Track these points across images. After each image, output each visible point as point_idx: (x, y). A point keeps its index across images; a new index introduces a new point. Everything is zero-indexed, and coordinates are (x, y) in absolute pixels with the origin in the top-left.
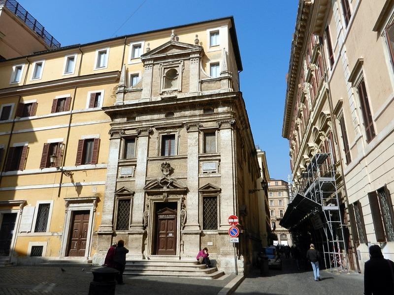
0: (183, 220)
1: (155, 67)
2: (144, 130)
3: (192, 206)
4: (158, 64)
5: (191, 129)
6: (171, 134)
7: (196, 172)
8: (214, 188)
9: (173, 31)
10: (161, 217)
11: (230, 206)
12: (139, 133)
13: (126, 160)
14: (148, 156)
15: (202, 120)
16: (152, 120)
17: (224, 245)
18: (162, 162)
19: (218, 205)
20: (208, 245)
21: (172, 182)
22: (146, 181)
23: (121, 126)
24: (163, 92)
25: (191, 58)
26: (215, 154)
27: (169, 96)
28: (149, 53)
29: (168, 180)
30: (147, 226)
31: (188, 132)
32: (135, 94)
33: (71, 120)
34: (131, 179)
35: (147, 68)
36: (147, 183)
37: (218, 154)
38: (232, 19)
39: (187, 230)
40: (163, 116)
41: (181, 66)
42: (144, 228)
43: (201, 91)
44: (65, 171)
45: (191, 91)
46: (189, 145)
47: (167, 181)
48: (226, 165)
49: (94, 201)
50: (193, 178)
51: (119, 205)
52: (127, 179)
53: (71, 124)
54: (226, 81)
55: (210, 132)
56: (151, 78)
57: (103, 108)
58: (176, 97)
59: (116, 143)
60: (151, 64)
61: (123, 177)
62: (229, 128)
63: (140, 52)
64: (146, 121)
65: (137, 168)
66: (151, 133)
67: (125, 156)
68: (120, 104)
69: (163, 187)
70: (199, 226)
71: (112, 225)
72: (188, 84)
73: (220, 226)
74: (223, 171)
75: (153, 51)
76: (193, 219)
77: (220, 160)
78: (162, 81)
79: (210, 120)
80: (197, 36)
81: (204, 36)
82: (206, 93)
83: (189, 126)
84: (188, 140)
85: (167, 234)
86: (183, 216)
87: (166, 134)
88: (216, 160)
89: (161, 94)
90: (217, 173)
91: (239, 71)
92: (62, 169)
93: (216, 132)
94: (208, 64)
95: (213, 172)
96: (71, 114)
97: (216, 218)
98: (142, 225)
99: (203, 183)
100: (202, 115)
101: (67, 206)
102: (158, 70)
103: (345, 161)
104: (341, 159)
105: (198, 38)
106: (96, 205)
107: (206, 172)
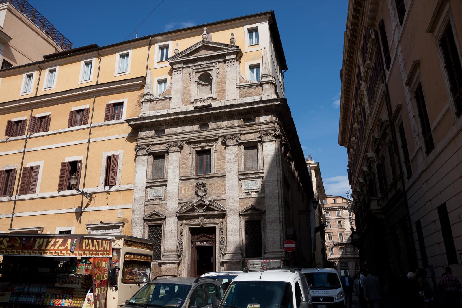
3: (232, 231)
4: (189, 67)
6: (206, 148)
7: (235, 192)
15: (241, 132)
16: (183, 133)
18: (196, 181)
21: (210, 204)
23: (148, 141)
24: (195, 100)
25: (227, 60)
27: (202, 104)
28: (177, 55)
29: (204, 202)
32: (162, 103)
34: (163, 202)
37: (262, 171)
38: (272, 14)
40: (196, 127)
41: (215, 69)
44: (87, 193)
45: (228, 98)
50: (233, 199)
51: (150, 231)
52: (157, 202)
53: (90, 139)
55: (251, 145)
57: (127, 121)
58: (210, 106)
59: (143, 160)
61: (152, 199)
64: (176, 134)
66: (181, 148)
68: (146, 115)
70: (241, 254)
72: (224, 90)
73: (265, 253)
75: (181, 53)
79: (251, 131)
84: (227, 155)
86: (222, 243)
87: (200, 149)
88: (259, 177)
91: (283, 71)
92: (83, 192)
96: (90, 128)
100: (242, 126)
103: (406, 175)
104: (402, 173)
107: (248, 192)
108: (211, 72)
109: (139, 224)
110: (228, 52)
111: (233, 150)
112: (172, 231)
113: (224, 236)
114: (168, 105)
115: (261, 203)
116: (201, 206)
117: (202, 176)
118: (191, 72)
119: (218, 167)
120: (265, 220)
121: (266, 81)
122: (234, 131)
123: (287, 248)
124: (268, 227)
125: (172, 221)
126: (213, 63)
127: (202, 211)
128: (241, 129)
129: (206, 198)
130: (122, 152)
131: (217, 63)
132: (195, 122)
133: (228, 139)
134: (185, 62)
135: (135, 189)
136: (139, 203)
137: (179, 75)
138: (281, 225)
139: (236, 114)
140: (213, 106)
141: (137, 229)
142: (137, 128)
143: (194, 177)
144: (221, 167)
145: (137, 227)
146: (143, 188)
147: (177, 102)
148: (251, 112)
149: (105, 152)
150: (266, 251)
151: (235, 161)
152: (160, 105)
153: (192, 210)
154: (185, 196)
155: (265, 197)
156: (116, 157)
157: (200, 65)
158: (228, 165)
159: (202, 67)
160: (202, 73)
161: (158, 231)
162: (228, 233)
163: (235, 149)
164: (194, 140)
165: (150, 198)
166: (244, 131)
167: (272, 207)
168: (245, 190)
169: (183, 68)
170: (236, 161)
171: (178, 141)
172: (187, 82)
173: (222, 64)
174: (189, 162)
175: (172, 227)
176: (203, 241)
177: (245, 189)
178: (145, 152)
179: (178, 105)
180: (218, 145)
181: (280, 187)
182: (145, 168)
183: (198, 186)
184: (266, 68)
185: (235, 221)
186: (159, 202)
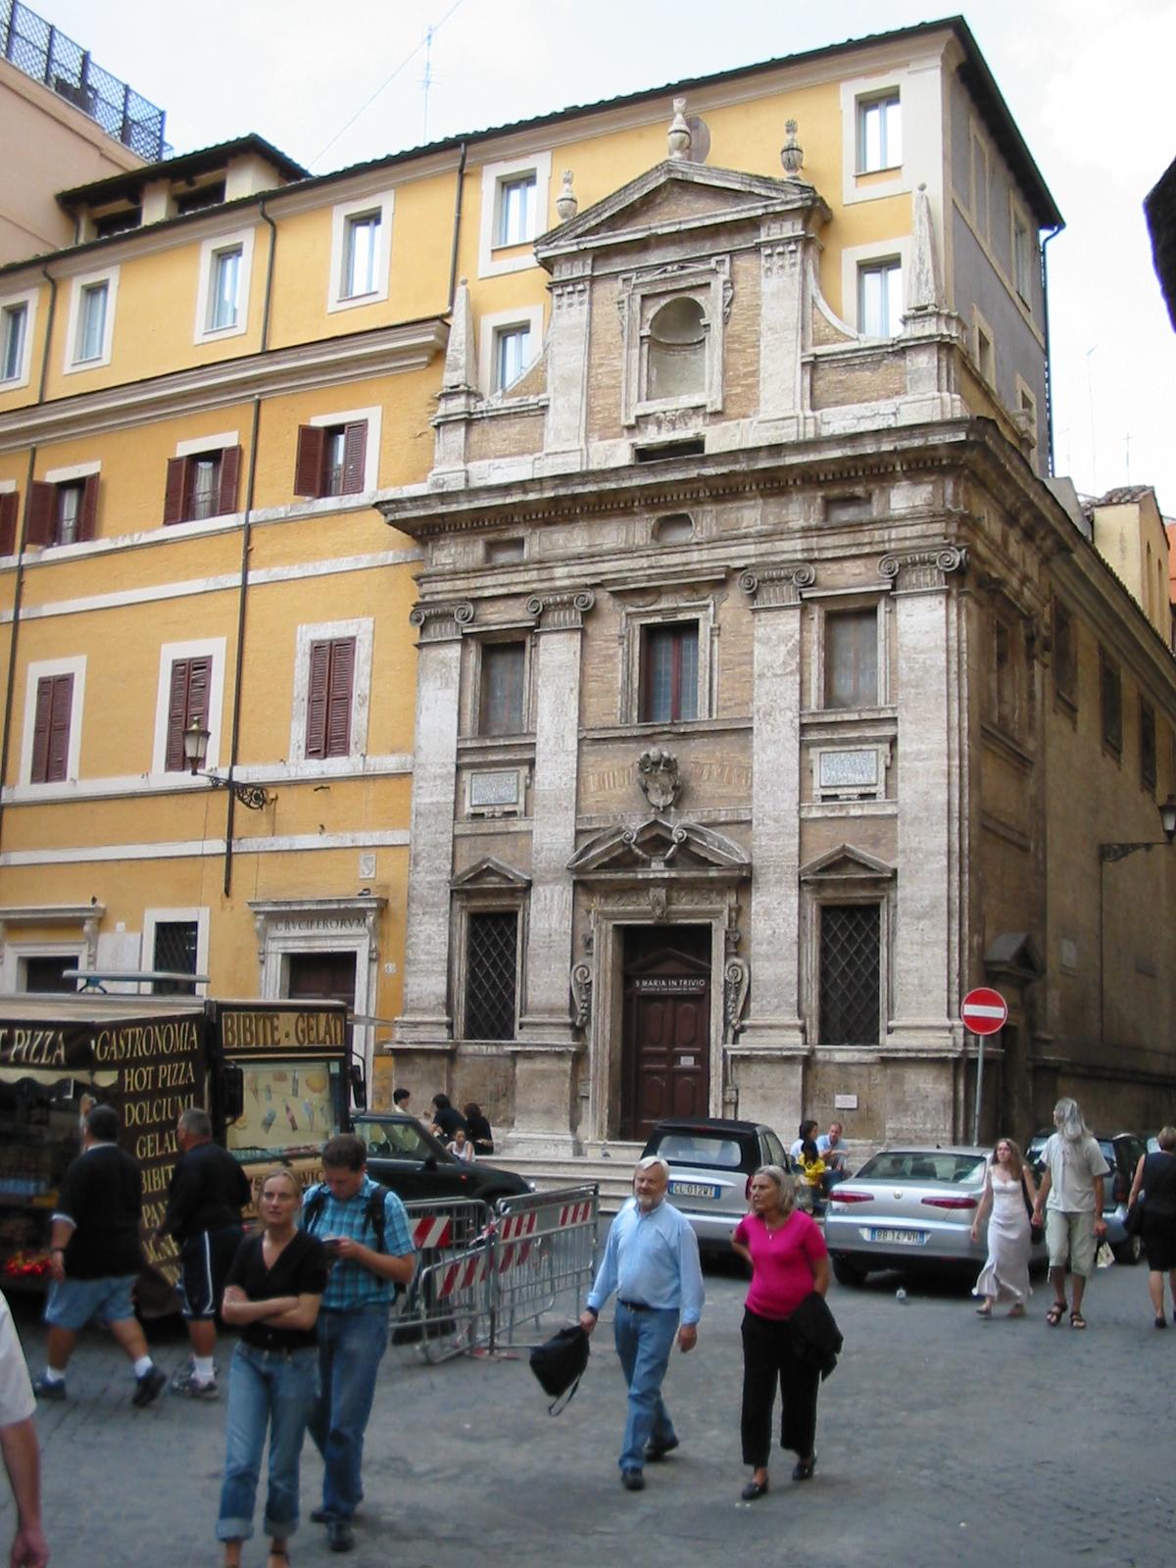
0: (735, 1001)
1: (602, 290)
3: (770, 943)
5: (769, 597)
6: (681, 617)
7: (787, 794)
8: (865, 867)
9: (678, 103)
10: (647, 986)
11: (936, 943)
12: (540, 616)
13: (494, 735)
14: (580, 723)
15: (816, 555)
16: (592, 557)
17: (901, 1107)
19: (883, 940)
20: (837, 1105)
22: (579, 833)
23: (460, 584)
25: (767, 244)
26: (875, 716)
27: (666, 436)
28: (573, 224)
29: (670, 830)
30: (588, 1022)
31: (754, 611)
32: (518, 428)
33: (247, 552)
34: (519, 825)
35: (565, 300)
36: (586, 842)
37: (888, 714)
38: (957, 28)
39: (748, 1042)
41: (717, 283)
42: (579, 1032)
43: (813, 408)
46: (757, 669)
48: (918, 764)
49: (370, 919)
50: (776, 820)
51: (473, 934)
52: (500, 825)
53: (251, 574)
54: (924, 362)
55: (852, 605)
56: (582, 347)
58: (696, 445)
59: (443, 663)
62: (937, 593)
63: (533, 213)
65: (542, 773)
66: (590, 613)
67: (484, 727)
69: (646, 863)
70: (803, 1030)
71: (445, 1019)
73: (890, 1031)
74: (906, 792)
77: (893, 742)
78: (635, 365)
79: (854, 551)
80: (791, 128)
81: (825, 119)
82: (840, 420)
84: (758, 648)
85: (676, 1058)
86: (731, 987)
88: (878, 740)
89: (630, 428)
91: (1044, 234)
94: (850, 256)
95: (863, 796)
97: (876, 996)
98: (569, 1020)
99: (819, 854)
100: (818, 530)
101: (262, 935)
102: (619, 307)
105: (800, 139)
106: (377, 933)
107: (835, 797)
108: (703, 298)
109: (435, 905)
110: (771, 210)
111: (781, 627)
112: (554, 937)
114: (537, 436)
115: (884, 841)
116: (655, 841)
117: (666, 729)
118: (624, 297)
119: (725, 696)
122: (785, 549)
124: (903, 933)
126: (710, 256)
127: (662, 866)
128: (814, 542)
130: (367, 623)
132: (635, 510)
133: (764, 581)
135: (418, 772)
136: (433, 829)
138: (955, 926)
139: (795, 481)
140: (710, 449)
141: (428, 927)
143: (635, 732)
144: (738, 694)
145: (427, 917)
146: (444, 771)
149: (304, 627)
151: (788, 670)
152: (504, 436)
153: (624, 859)
154: (599, 805)
155: (896, 816)
159: (668, 275)
160: (667, 300)
161: (502, 934)
163: (789, 623)
164: (632, 586)
165: (472, 811)
166: (827, 548)
167: (921, 856)
168: (822, 787)
169: (593, 280)
170: (791, 673)
171: (574, 588)
172: (609, 340)
174: (614, 670)
175: (555, 923)
177: (823, 784)
179: (570, 446)
180: (734, 597)
181: (955, 779)
182: (453, 694)
183: (648, 766)
184: (923, 278)
185: (783, 905)
186: (507, 826)
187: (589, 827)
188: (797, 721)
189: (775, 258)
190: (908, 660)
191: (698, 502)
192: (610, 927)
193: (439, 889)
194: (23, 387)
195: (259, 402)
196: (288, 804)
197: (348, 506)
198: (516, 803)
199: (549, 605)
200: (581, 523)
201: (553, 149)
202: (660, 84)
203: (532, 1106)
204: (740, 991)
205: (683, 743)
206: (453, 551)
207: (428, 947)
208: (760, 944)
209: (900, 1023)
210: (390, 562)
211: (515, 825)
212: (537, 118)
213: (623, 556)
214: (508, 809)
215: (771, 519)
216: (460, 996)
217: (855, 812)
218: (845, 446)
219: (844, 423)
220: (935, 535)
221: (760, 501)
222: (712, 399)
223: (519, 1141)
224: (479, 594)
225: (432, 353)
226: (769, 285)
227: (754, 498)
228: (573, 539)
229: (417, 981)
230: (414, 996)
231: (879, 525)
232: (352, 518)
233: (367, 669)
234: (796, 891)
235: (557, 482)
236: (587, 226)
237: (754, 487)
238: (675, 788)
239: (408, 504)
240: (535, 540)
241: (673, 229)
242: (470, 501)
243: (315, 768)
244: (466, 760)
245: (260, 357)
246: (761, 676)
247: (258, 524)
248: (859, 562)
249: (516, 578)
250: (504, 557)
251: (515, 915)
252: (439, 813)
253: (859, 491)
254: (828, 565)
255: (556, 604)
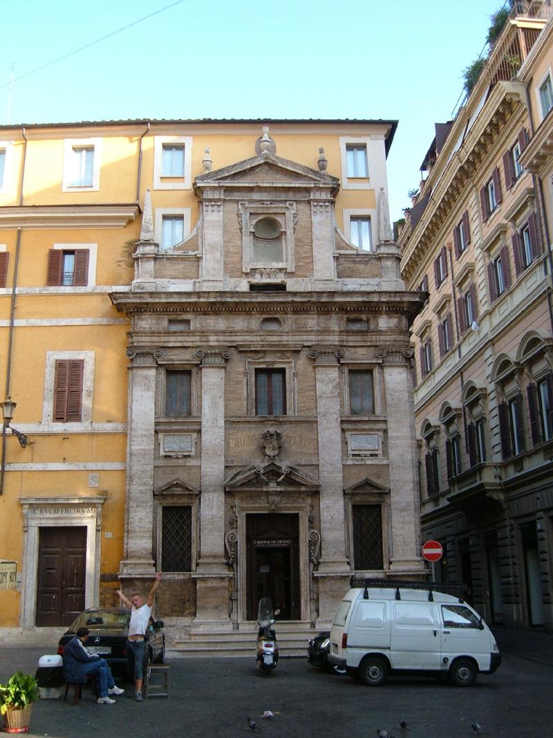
0: (314, 550)
2: (215, 354)
3: (330, 522)
5: (322, 360)
6: (276, 366)
7: (336, 453)
8: (377, 488)
11: (410, 523)
15: (345, 344)
23: (155, 339)
27: (265, 280)
29: (280, 468)
33: (13, 308)
34: (193, 462)
40: (255, 322)
41: (289, 214)
47: (275, 469)
50: (331, 465)
55: (361, 368)
58: (281, 288)
59: (146, 378)
60: (219, 200)
61: (170, 456)
62: (403, 366)
64: (217, 333)
65: (204, 437)
69: (267, 484)
71: (153, 562)
74: (393, 454)
76: (334, 550)
77: (385, 431)
79: (363, 344)
80: (321, 151)
82: (352, 284)
83: (315, 355)
86: (312, 544)
87: (264, 366)
88: (378, 430)
90: (380, 457)
93: (376, 372)
95: (371, 455)
99: (354, 482)
107: (359, 455)
109: (143, 502)
113: (316, 531)
116: (273, 472)
119: (301, 405)
120: (390, 505)
121: (388, 254)
123: (428, 556)
124: (394, 518)
125: (213, 500)
126: (286, 201)
129: (281, 460)
131: (295, 204)
134: (229, 190)
137: (215, 214)
140: (289, 289)
141: (140, 513)
142: (127, 309)
144: (307, 404)
145: (139, 509)
147: (214, 269)
148: (363, 309)
149: (51, 352)
150: (392, 560)
153: (256, 480)
155: (388, 465)
156: (77, 366)
157: (258, 201)
158: (321, 403)
162: (323, 525)
163: (334, 374)
164: (253, 349)
165: (164, 454)
170: (335, 397)
172: (233, 230)
173: (303, 208)
175: (215, 512)
176: (270, 539)
178: (149, 361)
179: (214, 277)
182: (151, 394)
186: (185, 463)
187: (232, 465)
188: (339, 419)
189: (318, 208)
190: (391, 395)
191: (286, 313)
192: (245, 514)
193: (146, 493)
194: (7, 196)
195: (19, 232)
196: (41, 443)
197: (79, 292)
198: (190, 451)
199: (207, 354)
200: (223, 316)
201: (193, 136)
202: (255, 118)
203: (206, 605)
204: (316, 544)
205: (280, 426)
206: (150, 322)
207: (140, 524)
208: (326, 523)
209: (397, 559)
210: (105, 323)
211: (190, 462)
212: (319, 120)
213: (247, 334)
214: (185, 454)
215: (322, 325)
216: (159, 549)
217: (369, 462)
218: (364, 297)
219: (354, 286)
220: (400, 341)
221: (316, 316)
222: (291, 267)
223: (201, 624)
224: (166, 345)
225: (127, 220)
226: (316, 219)
227: (313, 314)
228: (219, 323)
229: (134, 542)
230: (133, 550)
231: (375, 333)
232: (79, 299)
233: (91, 377)
234: (342, 498)
235: (217, 295)
236: (223, 176)
237: (315, 309)
238: (280, 447)
239: (131, 295)
240: (197, 321)
241: (268, 185)
242: (167, 298)
243: (60, 427)
244: (159, 427)
245: (31, 208)
246: (320, 397)
247: (21, 295)
248: (364, 349)
249: (187, 339)
250: (174, 328)
251: (190, 508)
252: (145, 454)
253: (364, 317)
254: (350, 349)
255: (212, 354)
